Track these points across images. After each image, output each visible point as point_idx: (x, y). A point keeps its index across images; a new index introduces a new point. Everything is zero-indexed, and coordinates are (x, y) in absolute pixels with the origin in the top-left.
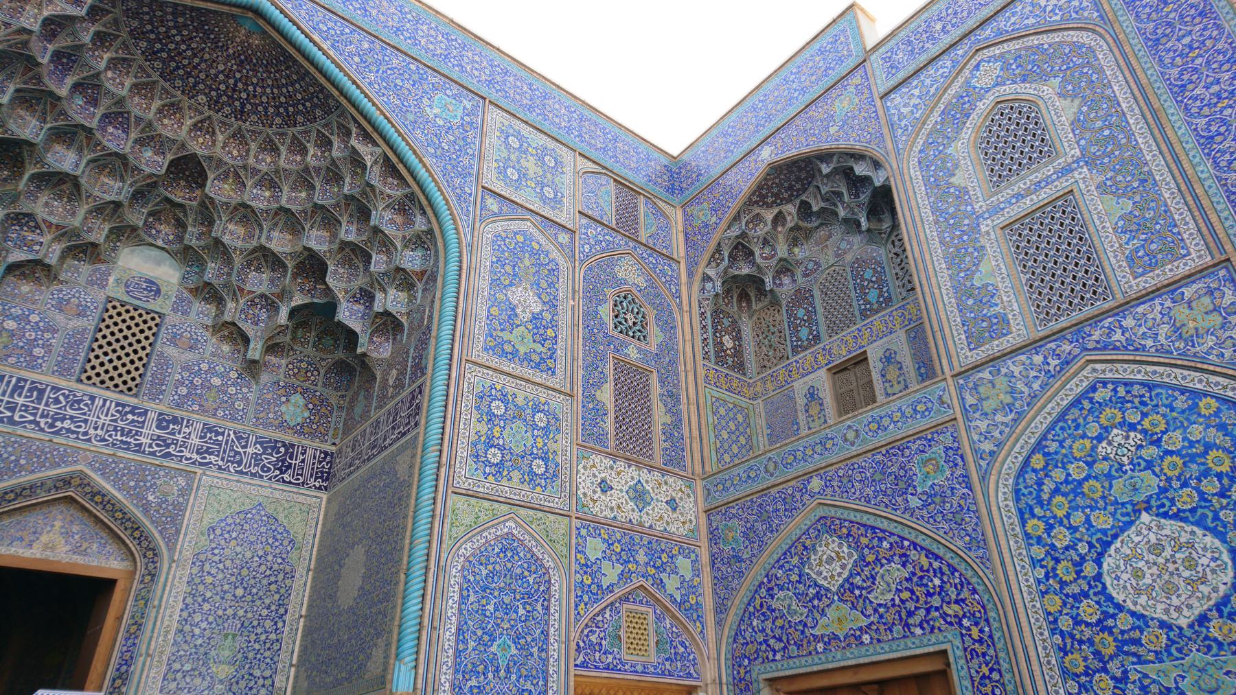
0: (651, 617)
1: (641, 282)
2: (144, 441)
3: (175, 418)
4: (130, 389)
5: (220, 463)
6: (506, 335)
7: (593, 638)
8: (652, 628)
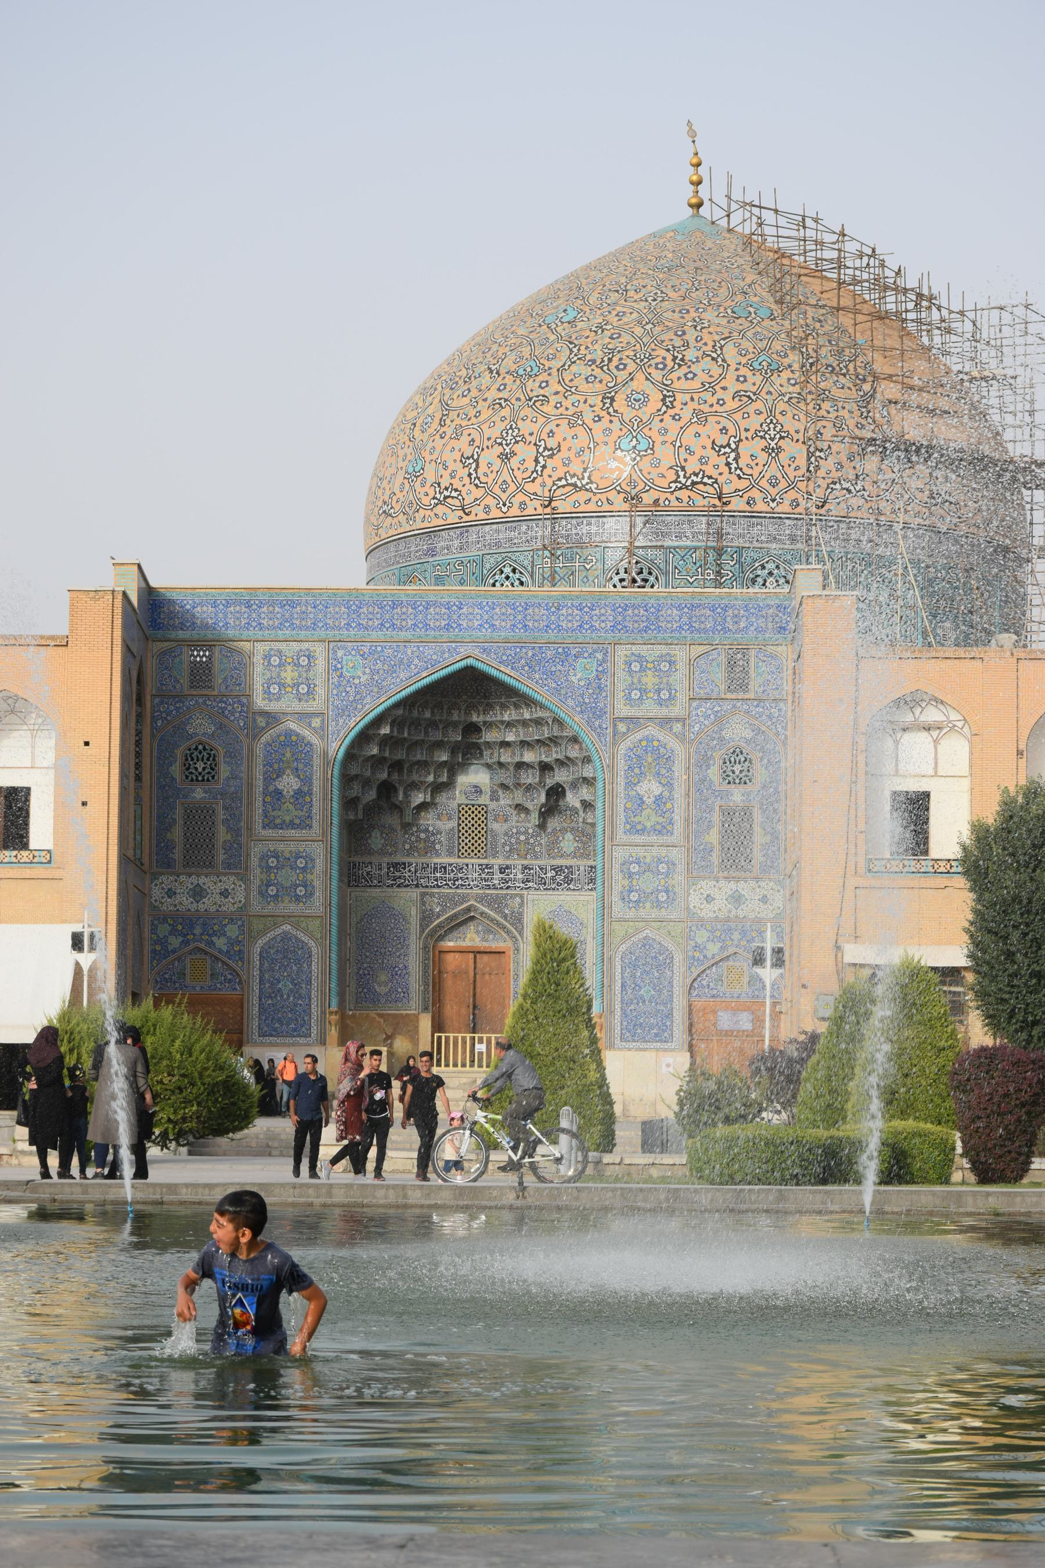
1: (748, 734)
2: (496, 882)
6: (636, 819)
7: (704, 983)
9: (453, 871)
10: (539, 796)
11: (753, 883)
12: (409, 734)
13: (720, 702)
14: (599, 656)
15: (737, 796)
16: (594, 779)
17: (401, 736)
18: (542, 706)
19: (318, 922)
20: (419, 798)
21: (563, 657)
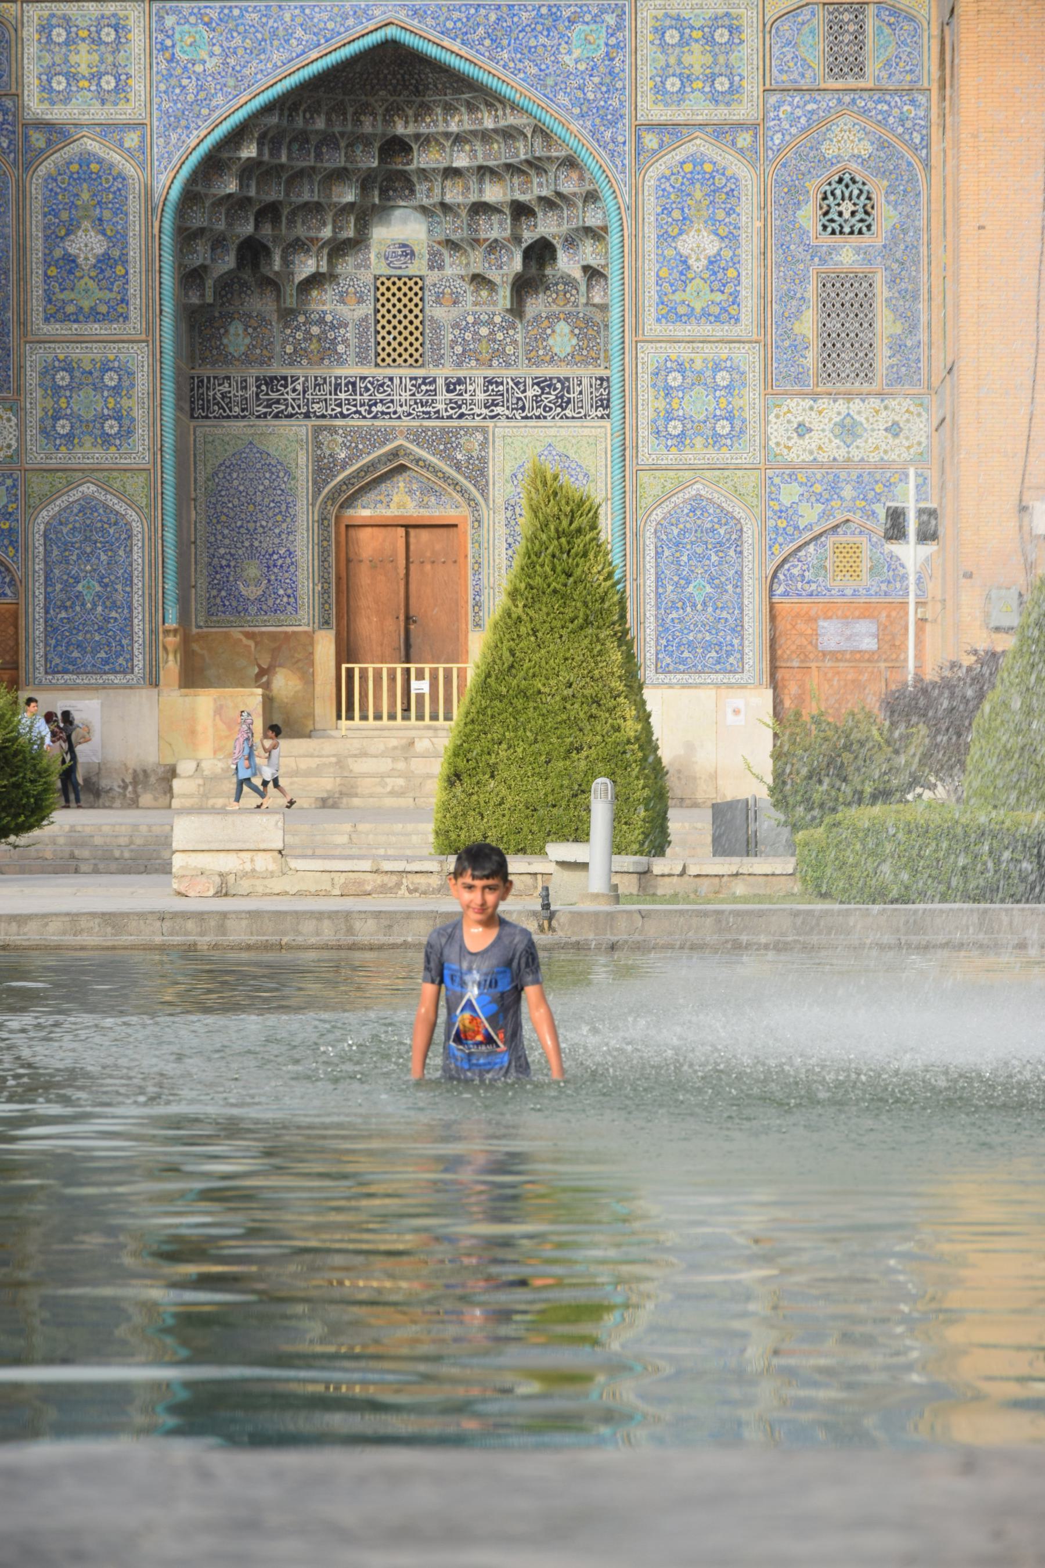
0: (866, 546)
1: (865, 148)
2: (441, 406)
3: (459, 379)
4: (416, 361)
5: (507, 412)
6: (678, 297)
7: (796, 571)
8: (866, 554)
9: (367, 390)
10: (511, 259)
11: (875, 402)
12: (289, 158)
13: (815, 94)
14: (610, 19)
15: (847, 254)
16: (605, 229)
17: (277, 161)
18: (515, 107)
19: (141, 479)
20: (307, 266)
21: (548, 22)
